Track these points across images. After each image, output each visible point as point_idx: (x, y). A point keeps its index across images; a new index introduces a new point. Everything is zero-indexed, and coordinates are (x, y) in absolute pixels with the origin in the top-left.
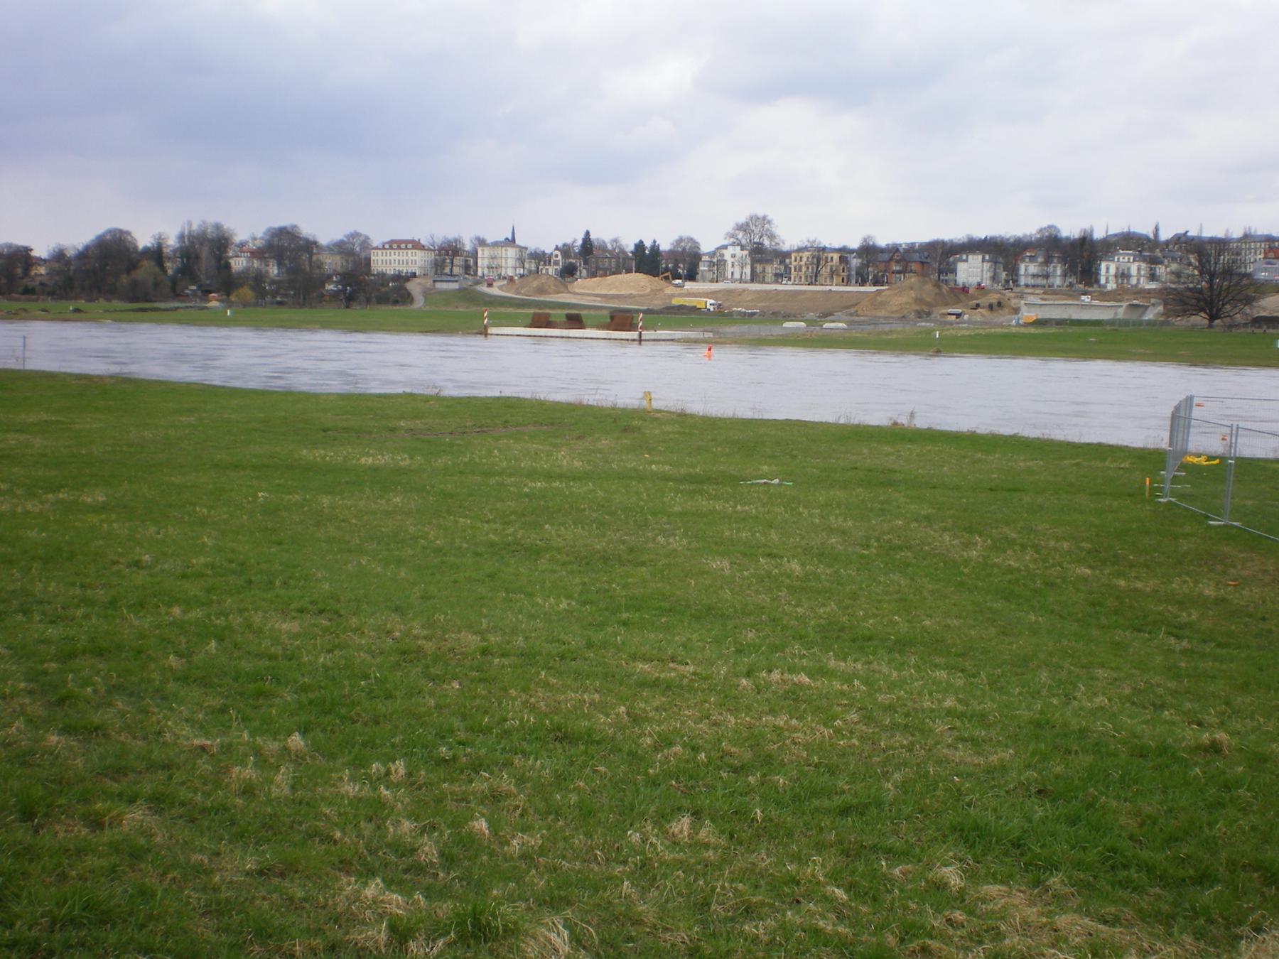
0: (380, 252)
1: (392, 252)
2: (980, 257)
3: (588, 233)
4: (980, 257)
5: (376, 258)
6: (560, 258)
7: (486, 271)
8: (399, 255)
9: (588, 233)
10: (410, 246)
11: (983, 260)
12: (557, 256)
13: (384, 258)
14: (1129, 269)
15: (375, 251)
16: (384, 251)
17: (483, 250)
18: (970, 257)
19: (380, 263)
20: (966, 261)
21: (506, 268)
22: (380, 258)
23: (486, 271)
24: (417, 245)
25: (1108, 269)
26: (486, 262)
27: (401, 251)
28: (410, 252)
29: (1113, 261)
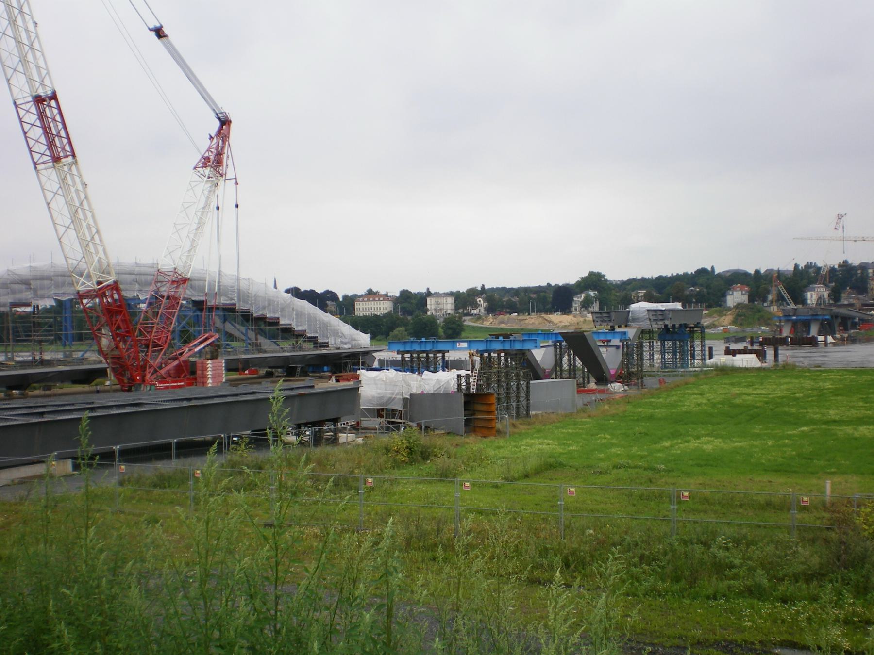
0: (361, 303)
1: (370, 303)
2: (740, 292)
3: (483, 285)
4: (740, 292)
5: (358, 307)
6: (482, 302)
7: (433, 312)
8: (374, 304)
9: (483, 285)
10: (381, 299)
11: (742, 294)
12: (480, 301)
13: (364, 307)
14: (823, 296)
15: (358, 303)
16: (364, 303)
17: (431, 300)
18: (734, 292)
19: (361, 309)
20: (732, 294)
21: (447, 310)
22: (361, 307)
23: (433, 312)
24: (386, 297)
25: (812, 295)
26: (433, 307)
27: (376, 302)
28: (382, 302)
29: (814, 291)
